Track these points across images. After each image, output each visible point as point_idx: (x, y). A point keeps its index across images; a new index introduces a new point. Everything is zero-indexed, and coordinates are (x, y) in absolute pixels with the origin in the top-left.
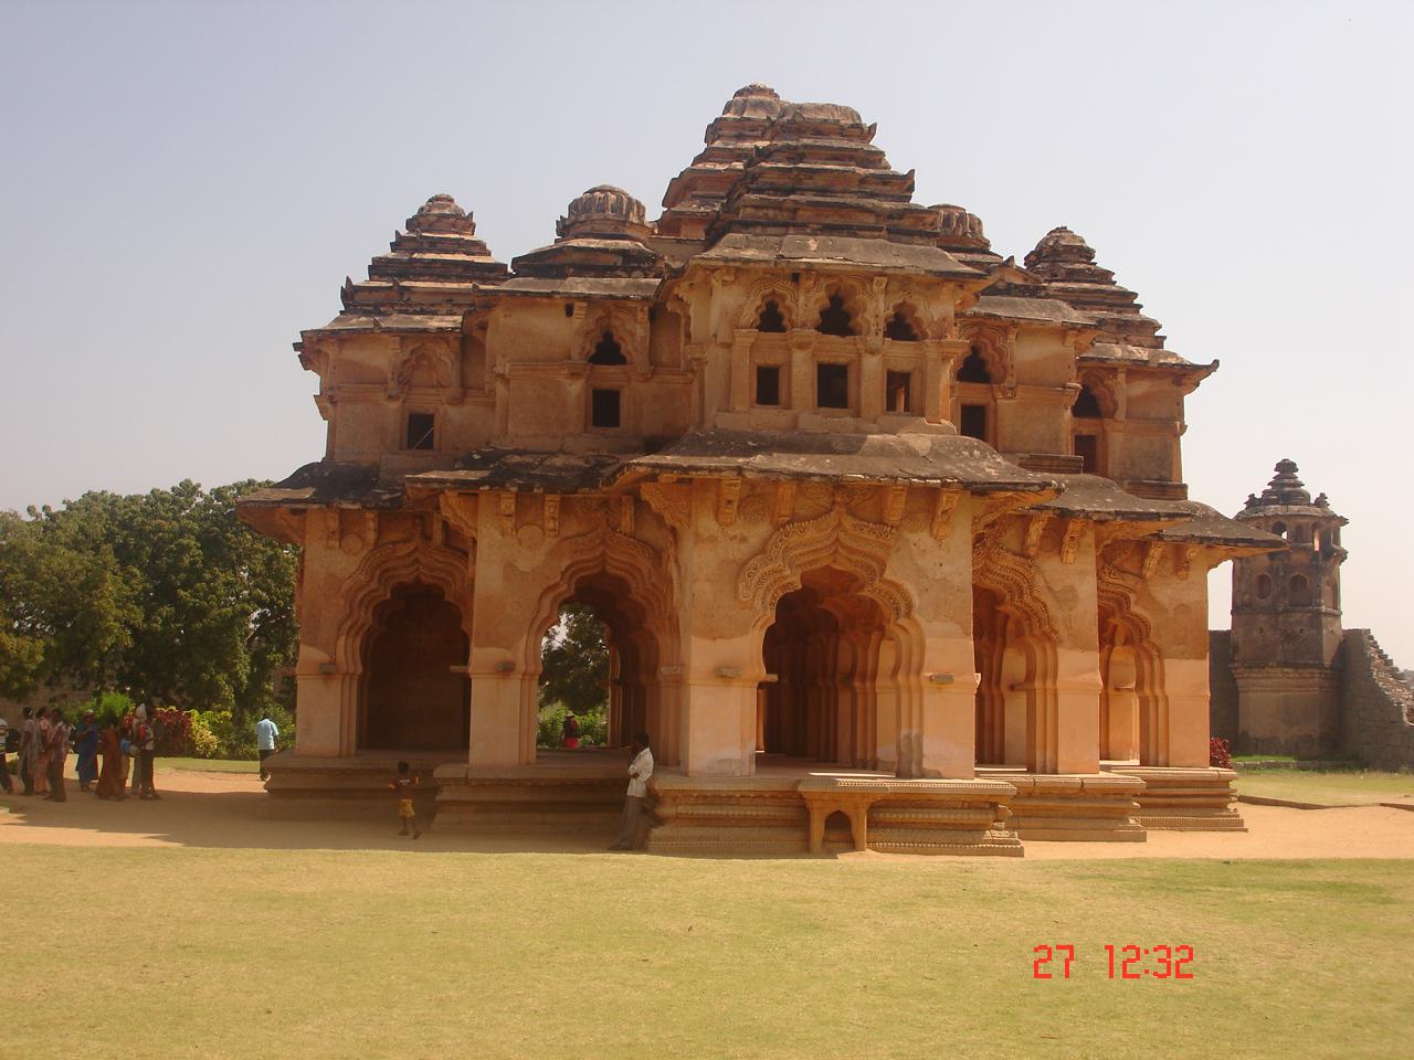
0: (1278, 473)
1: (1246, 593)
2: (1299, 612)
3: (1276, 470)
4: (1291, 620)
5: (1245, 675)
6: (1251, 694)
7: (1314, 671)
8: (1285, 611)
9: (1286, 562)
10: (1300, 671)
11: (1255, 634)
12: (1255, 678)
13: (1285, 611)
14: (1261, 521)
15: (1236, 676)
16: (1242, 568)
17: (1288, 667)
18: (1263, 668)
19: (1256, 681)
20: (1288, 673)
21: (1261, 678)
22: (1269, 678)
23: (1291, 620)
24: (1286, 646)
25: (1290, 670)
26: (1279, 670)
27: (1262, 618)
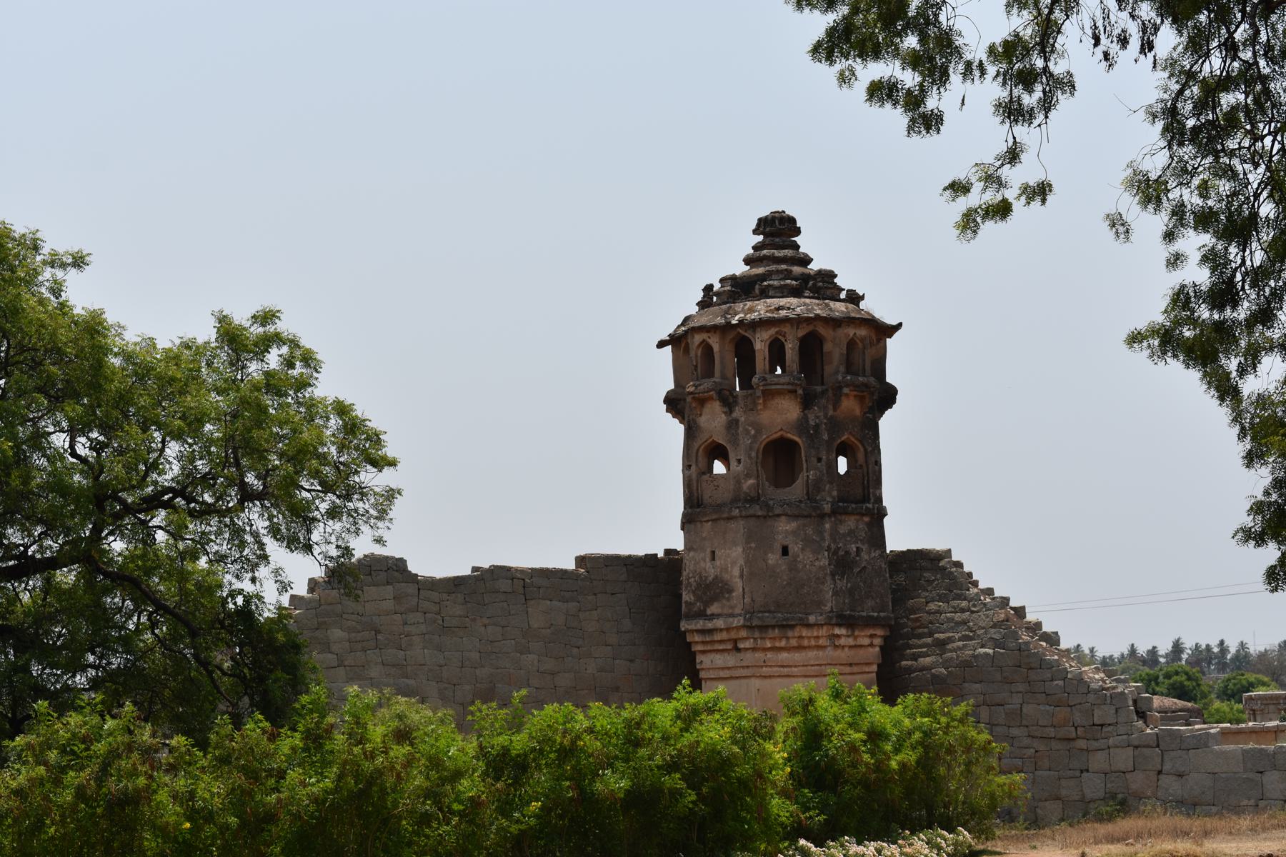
0: (760, 238)
1: (748, 476)
2: (852, 514)
3: (755, 232)
4: (843, 529)
7: (880, 632)
8: (834, 513)
9: (831, 413)
11: (773, 558)
12: (772, 649)
13: (834, 513)
14: (787, 329)
17: (839, 625)
18: (792, 627)
19: (769, 655)
20: (839, 636)
22: (800, 648)
23: (843, 529)
25: (842, 631)
26: (823, 632)
27: (784, 527)
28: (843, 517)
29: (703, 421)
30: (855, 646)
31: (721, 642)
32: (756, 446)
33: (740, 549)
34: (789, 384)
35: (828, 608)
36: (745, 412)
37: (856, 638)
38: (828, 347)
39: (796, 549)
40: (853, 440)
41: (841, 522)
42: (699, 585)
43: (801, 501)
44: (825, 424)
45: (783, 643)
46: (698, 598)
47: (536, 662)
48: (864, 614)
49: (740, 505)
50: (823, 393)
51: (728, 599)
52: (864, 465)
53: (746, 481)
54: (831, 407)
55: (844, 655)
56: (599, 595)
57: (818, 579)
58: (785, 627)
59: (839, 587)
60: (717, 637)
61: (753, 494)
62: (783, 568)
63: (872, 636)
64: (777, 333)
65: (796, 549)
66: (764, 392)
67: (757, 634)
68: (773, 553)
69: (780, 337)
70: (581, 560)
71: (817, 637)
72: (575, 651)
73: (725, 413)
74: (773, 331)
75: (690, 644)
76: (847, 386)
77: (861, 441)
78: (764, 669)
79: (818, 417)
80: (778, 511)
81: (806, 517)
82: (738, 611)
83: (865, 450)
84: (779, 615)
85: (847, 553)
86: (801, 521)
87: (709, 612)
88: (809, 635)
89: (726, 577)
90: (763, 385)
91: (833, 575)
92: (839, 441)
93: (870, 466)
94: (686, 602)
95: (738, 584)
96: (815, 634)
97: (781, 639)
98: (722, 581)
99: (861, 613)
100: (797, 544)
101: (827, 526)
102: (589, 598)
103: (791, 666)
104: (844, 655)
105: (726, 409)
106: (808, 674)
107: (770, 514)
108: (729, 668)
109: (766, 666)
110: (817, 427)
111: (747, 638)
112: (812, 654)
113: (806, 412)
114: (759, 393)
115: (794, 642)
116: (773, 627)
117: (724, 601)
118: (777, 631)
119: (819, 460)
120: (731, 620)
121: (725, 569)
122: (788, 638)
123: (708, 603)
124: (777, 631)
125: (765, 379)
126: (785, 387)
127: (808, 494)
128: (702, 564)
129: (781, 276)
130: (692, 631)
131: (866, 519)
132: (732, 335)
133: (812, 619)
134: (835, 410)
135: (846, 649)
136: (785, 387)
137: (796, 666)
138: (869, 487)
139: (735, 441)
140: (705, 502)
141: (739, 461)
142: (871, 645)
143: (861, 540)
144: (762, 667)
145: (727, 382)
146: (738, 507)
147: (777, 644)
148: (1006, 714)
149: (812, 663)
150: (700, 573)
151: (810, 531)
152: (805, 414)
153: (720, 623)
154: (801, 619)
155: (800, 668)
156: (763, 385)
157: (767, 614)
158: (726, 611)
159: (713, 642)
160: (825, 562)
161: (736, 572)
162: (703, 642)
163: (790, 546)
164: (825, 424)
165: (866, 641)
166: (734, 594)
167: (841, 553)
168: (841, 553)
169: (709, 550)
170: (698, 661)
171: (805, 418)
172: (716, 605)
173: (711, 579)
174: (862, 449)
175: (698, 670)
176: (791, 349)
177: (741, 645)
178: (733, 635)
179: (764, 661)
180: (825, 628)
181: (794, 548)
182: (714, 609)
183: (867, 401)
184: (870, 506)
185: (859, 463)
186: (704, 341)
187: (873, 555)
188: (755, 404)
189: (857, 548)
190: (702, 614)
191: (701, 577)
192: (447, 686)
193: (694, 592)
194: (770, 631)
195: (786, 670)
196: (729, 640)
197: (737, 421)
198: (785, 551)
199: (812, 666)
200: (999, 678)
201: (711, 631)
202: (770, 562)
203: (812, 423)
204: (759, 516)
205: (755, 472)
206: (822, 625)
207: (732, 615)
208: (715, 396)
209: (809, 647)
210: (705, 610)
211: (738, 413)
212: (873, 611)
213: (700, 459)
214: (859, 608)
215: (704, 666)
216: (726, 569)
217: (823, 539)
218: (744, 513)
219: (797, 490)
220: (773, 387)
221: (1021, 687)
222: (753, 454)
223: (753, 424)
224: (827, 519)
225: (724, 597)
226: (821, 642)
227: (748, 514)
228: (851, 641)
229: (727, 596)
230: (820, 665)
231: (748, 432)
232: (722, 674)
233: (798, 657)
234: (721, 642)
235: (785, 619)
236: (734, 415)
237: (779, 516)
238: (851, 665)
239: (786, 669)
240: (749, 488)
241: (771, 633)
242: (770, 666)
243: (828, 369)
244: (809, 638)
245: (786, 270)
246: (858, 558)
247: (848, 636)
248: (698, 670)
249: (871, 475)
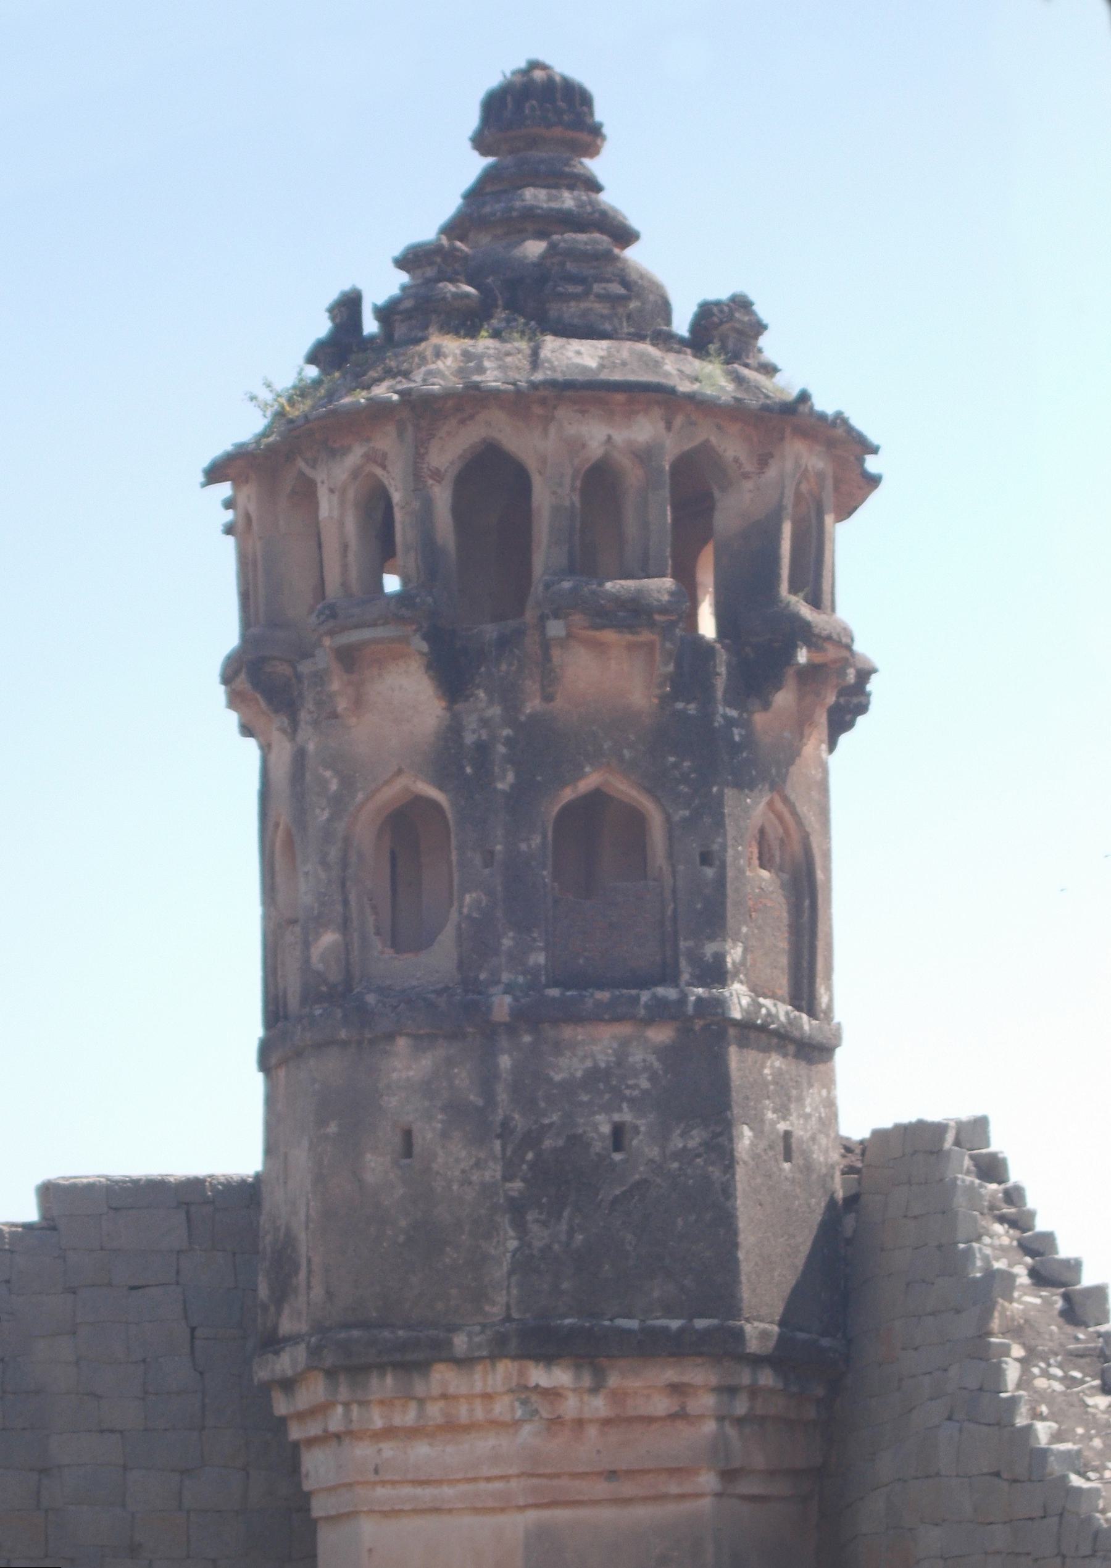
5: (336, 1421)
12: (389, 1432)
18: (423, 1367)
19: (389, 1449)
21: (413, 1433)
22: (452, 1428)
35: (496, 1311)
39: (429, 1135)
45: (408, 1417)
59: (538, 1244)
62: (400, 1191)
65: (429, 1135)
70: (49, 1192)
71: (488, 1397)
84: (386, 1334)
85: (576, 1141)
88: (464, 1390)
91: (517, 1209)
96: (478, 1387)
103: (439, 1482)
106: (480, 1505)
109: (383, 1483)
112: (485, 1444)
115: (435, 1411)
118: (389, 1380)
122: (421, 1402)
124: (389, 1380)
137: (452, 1482)
144: (375, 1483)
147: (398, 1420)
149: (486, 1471)
157: (356, 1333)
160: (494, 1172)
163: (415, 1128)
167: (548, 1143)
168: (548, 1143)
179: (376, 1471)
199: (488, 1479)
202: (370, 1178)
226: (501, 1408)
242: (393, 1483)
244: (470, 1398)
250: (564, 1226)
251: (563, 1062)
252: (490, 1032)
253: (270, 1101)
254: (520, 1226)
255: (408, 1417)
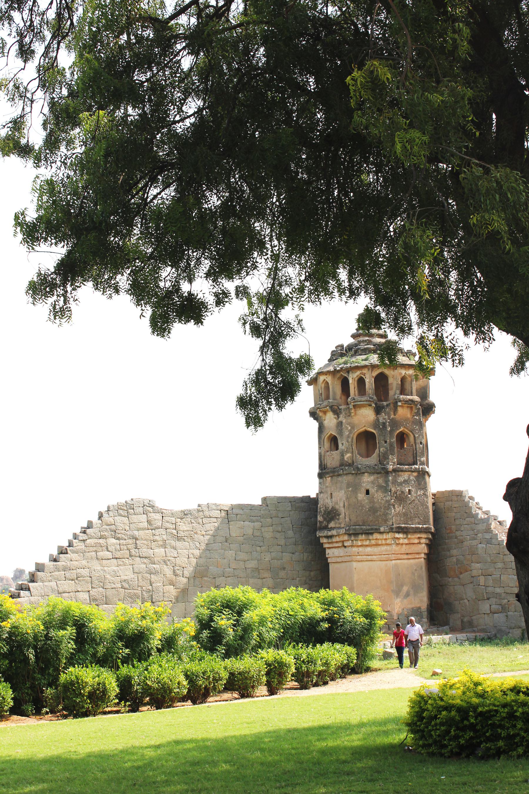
1: (347, 452)
4: (401, 479)
6: (355, 564)
7: (424, 536)
9: (392, 416)
10: (409, 536)
11: (361, 496)
12: (361, 546)
14: (365, 371)
15: (326, 546)
16: (340, 424)
17: (399, 532)
18: (372, 534)
19: (361, 549)
21: (367, 546)
22: (377, 545)
23: (401, 479)
24: (397, 509)
25: (401, 535)
26: (390, 535)
27: (367, 480)
28: (400, 473)
29: (326, 423)
30: (410, 544)
31: (337, 542)
32: (351, 435)
33: (343, 492)
34: (366, 401)
36: (345, 417)
37: (409, 539)
38: (391, 380)
40: (407, 431)
41: (399, 476)
42: (325, 511)
43: (376, 465)
44: (389, 422)
45: (367, 543)
46: (325, 519)
47: (234, 555)
48: (414, 526)
49: (343, 467)
50: (387, 405)
51: (338, 519)
52: (414, 445)
53: (346, 454)
54: (392, 413)
55: (404, 549)
56: (274, 518)
57: (385, 507)
58: (368, 533)
60: (334, 540)
61: (350, 461)
63: (419, 538)
64: (361, 373)
66: (354, 406)
67: (353, 538)
68: (361, 493)
69: (363, 376)
70: (264, 499)
71: (386, 539)
72: (258, 548)
73: (335, 418)
74: (358, 373)
75: (322, 544)
76: (400, 401)
77: (411, 432)
78: (358, 557)
79: (384, 419)
80: (363, 471)
81: (378, 473)
82: (342, 526)
83: (414, 436)
84: (364, 527)
86: (376, 476)
87: (329, 526)
89: (337, 507)
90: (353, 402)
92: (398, 432)
93: (417, 445)
94: (319, 521)
95: (342, 510)
96: (385, 537)
97: (366, 540)
98: (335, 509)
99: (412, 526)
100: (374, 488)
101: (390, 478)
102: (268, 520)
104: (404, 549)
105: (336, 416)
107: (359, 472)
108: (341, 557)
110: (384, 424)
111: (348, 540)
112: (384, 548)
113: (378, 416)
114: (351, 406)
115: (373, 542)
116: (362, 534)
117: (336, 521)
118: (364, 536)
119: (386, 442)
120: (339, 530)
121: (336, 503)
123: (329, 522)
124: (364, 536)
125: (354, 399)
126: (365, 403)
127: (379, 461)
128: (326, 501)
129: (365, 343)
130: (322, 537)
131: (415, 474)
132: (338, 375)
133: (382, 529)
134: (395, 415)
135: (404, 546)
136: (365, 403)
138: (416, 456)
139: (341, 432)
140: (328, 467)
141: (343, 444)
142: (420, 543)
143: (411, 486)
145: (336, 401)
146: (342, 469)
148: (493, 580)
149: (384, 553)
150: (325, 506)
151: (381, 481)
152: (377, 418)
153: (334, 532)
154: (376, 529)
155: (378, 556)
156: (353, 402)
157: (357, 527)
158: (337, 526)
159: (332, 543)
161: (342, 505)
162: (329, 543)
163: (370, 490)
164: (389, 422)
165: (416, 541)
166: (341, 516)
169: (329, 493)
170: (327, 553)
171: (378, 420)
172: (333, 522)
173: (330, 508)
174: (412, 436)
175: (327, 558)
176: (369, 382)
177: (346, 544)
178: (341, 538)
180: (390, 534)
181: (372, 491)
182: (332, 525)
183: (414, 409)
184: (417, 467)
185: (411, 444)
186: (325, 380)
187: (419, 493)
188: (350, 413)
189: (409, 490)
190: (326, 528)
191: (326, 508)
192: (179, 568)
193: (323, 516)
194: (360, 536)
195: (369, 558)
196: (340, 542)
197: (341, 423)
198: (368, 492)
200: (489, 560)
201: (331, 537)
202: (359, 498)
203: (381, 421)
204: (353, 474)
205: (351, 450)
206: (388, 532)
207: (339, 528)
208: (329, 410)
209: (382, 545)
210: (328, 526)
211: (342, 418)
212: (419, 524)
213: (325, 443)
214: (410, 523)
215: (329, 556)
216: (337, 503)
217: (388, 485)
218: (345, 472)
219: (373, 460)
220: (359, 403)
221: (500, 565)
222: (350, 440)
223: (349, 424)
224: (390, 474)
225: (336, 518)
227: (347, 473)
228: (406, 541)
229: (337, 517)
230: (389, 554)
231: (347, 428)
232: (339, 560)
233: (376, 550)
234: (337, 542)
235: (369, 530)
236: (340, 419)
237: (364, 473)
238: (407, 554)
239: (370, 557)
240: (347, 458)
241: (360, 537)
243: (391, 393)
245: (368, 340)
246: (409, 496)
247: (405, 538)
248: (327, 558)
249: (418, 450)
250: (401, 508)
251: (400, 478)
252: (387, 473)
253: (320, 483)
254: (394, 508)
255: (367, 543)
